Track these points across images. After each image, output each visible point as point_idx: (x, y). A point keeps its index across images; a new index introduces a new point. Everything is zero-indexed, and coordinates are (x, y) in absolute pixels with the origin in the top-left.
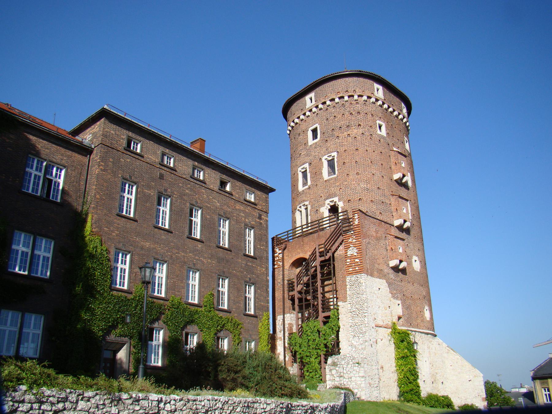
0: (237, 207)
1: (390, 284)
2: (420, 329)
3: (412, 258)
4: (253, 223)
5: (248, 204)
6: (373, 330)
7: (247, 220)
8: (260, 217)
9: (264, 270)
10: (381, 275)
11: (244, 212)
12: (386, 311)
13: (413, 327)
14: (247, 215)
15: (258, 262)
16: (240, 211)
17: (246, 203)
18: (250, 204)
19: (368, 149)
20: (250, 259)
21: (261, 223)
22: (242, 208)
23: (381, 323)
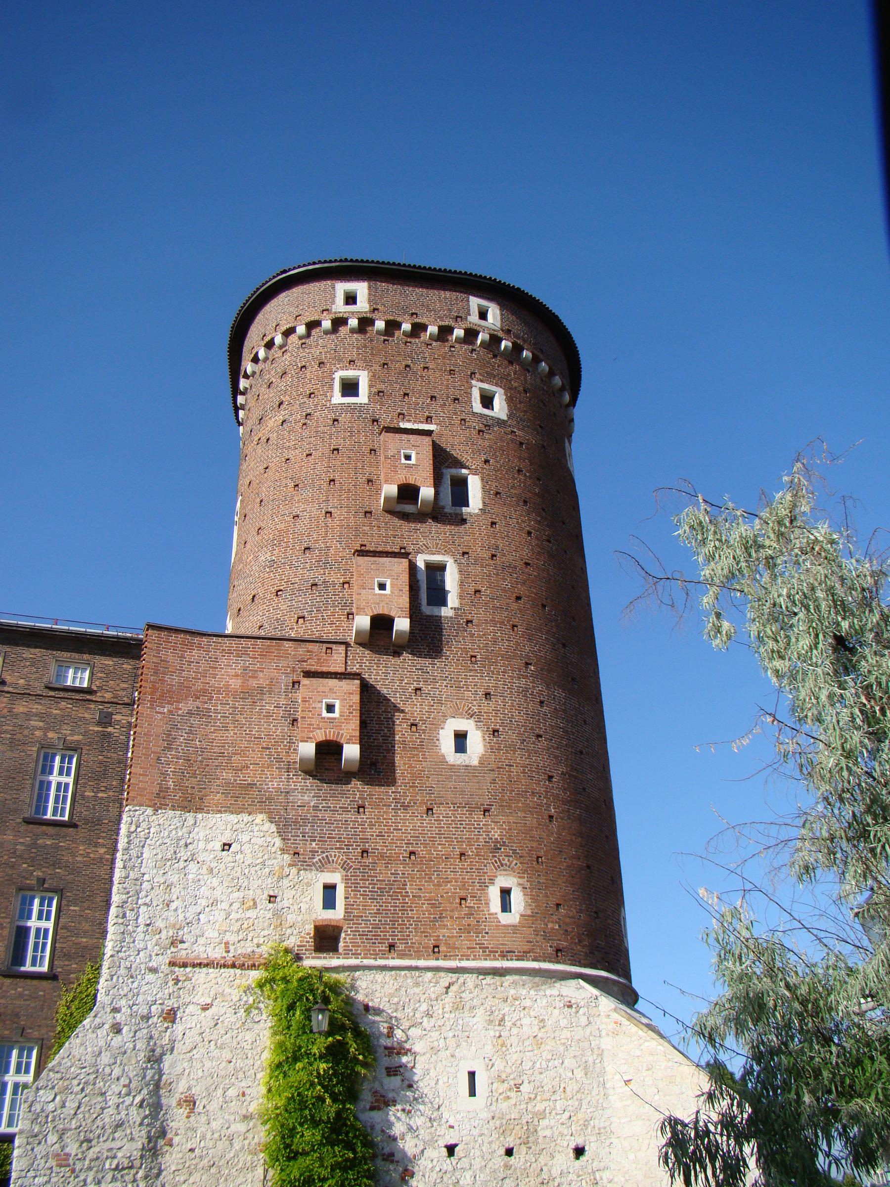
0: (21, 709)
1: (285, 826)
2: (446, 957)
3: (438, 725)
4: (76, 738)
5: (62, 694)
6: (150, 977)
7: (51, 735)
8: (106, 720)
9: (102, 850)
10: (243, 798)
11: (41, 716)
12: (251, 914)
13: (402, 956)
14: (52, 723)
15: (82, 832)
16: (28, 716)
17: (52, 693)
18: (66, 695)
19: (291, 454)
20: (51, 830)
21: (110, 734)
22: (37, 708)
23: (217, 953)
